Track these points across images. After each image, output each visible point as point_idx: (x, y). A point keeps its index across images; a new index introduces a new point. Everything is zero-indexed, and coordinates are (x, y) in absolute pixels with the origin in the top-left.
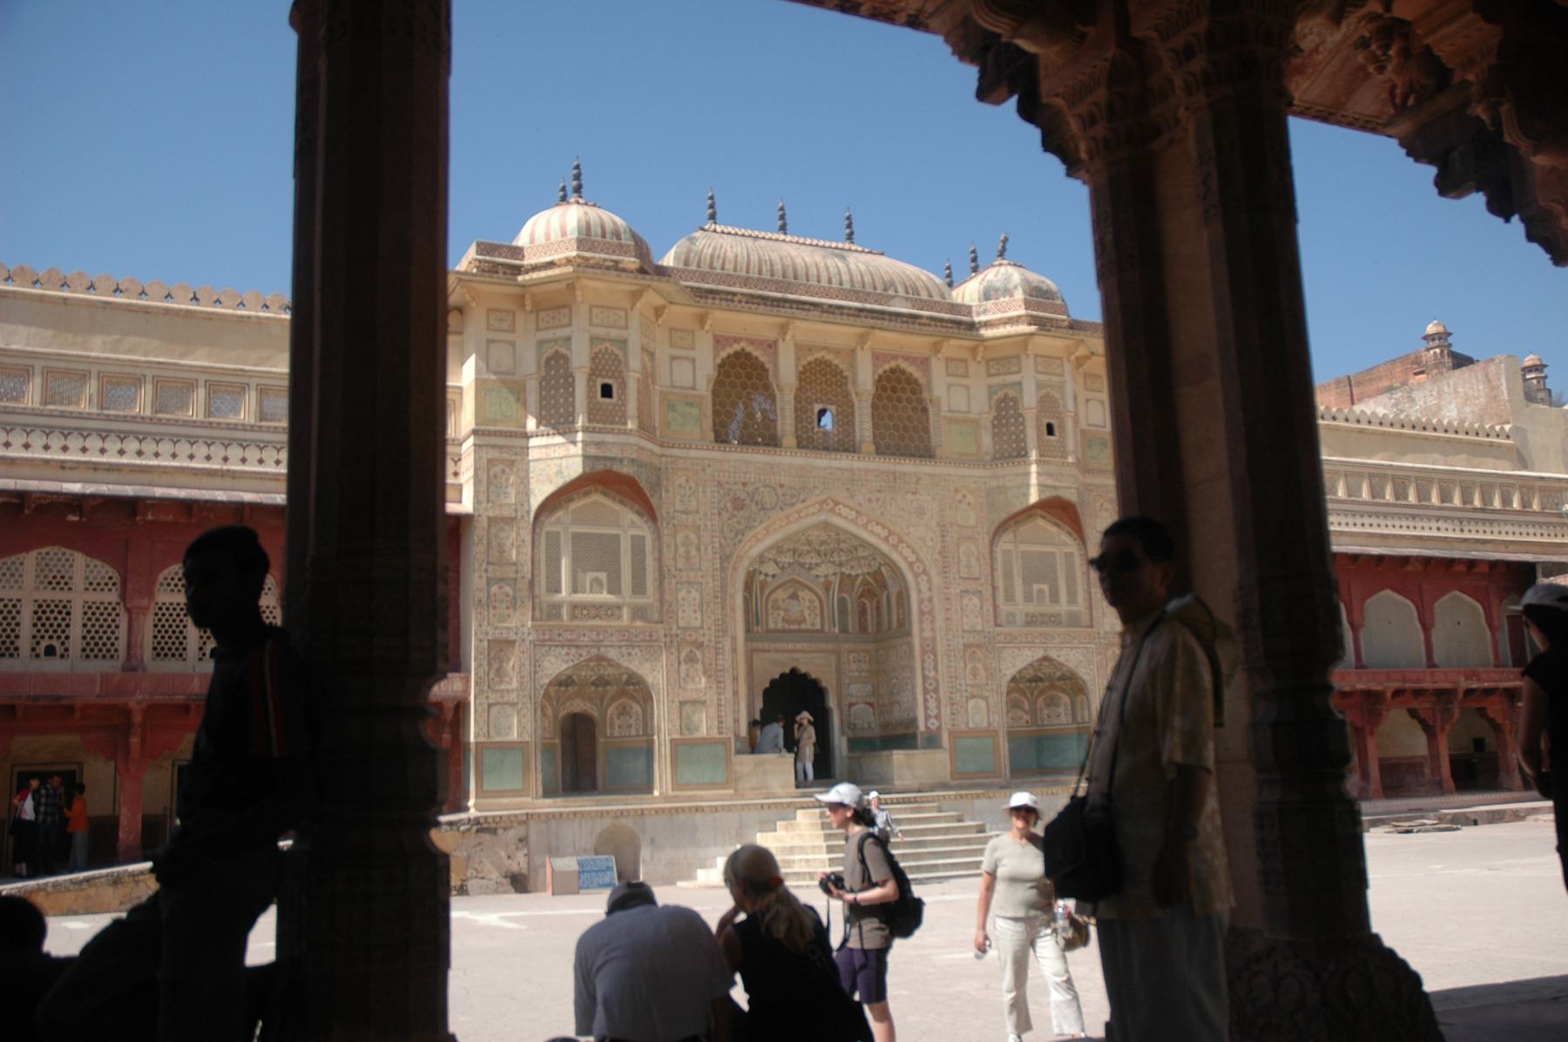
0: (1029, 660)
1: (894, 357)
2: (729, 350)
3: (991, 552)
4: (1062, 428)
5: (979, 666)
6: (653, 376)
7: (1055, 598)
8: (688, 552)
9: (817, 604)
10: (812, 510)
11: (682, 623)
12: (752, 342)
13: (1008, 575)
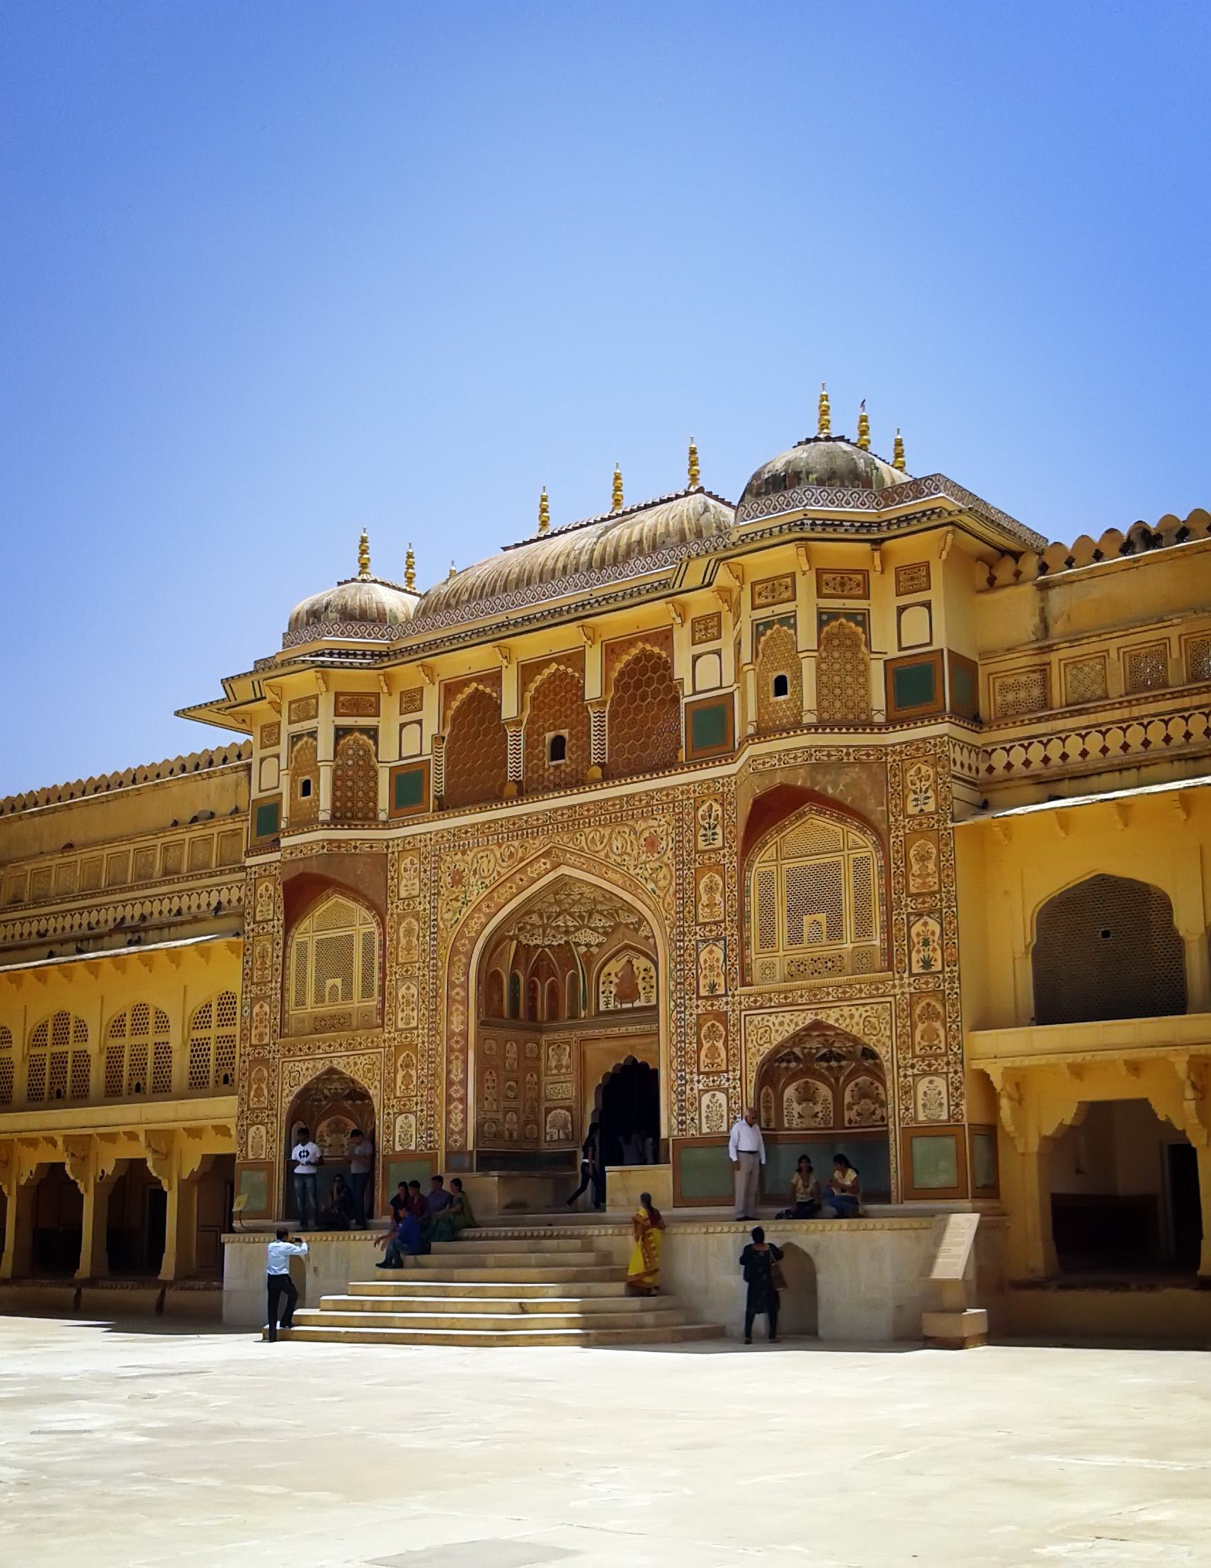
0: (791, 1031)
1: (631, 643)
2: (460, 697)
3: (742, 882)
4: (798, 677)
5: (720, 1044)
6: (376, 756)
7: (835, 931)
8: (409, 942)
9: (653, 973)
10: (541, 866)
11: (401, 1025)
12: (479, 680)
13: (767, 908)
